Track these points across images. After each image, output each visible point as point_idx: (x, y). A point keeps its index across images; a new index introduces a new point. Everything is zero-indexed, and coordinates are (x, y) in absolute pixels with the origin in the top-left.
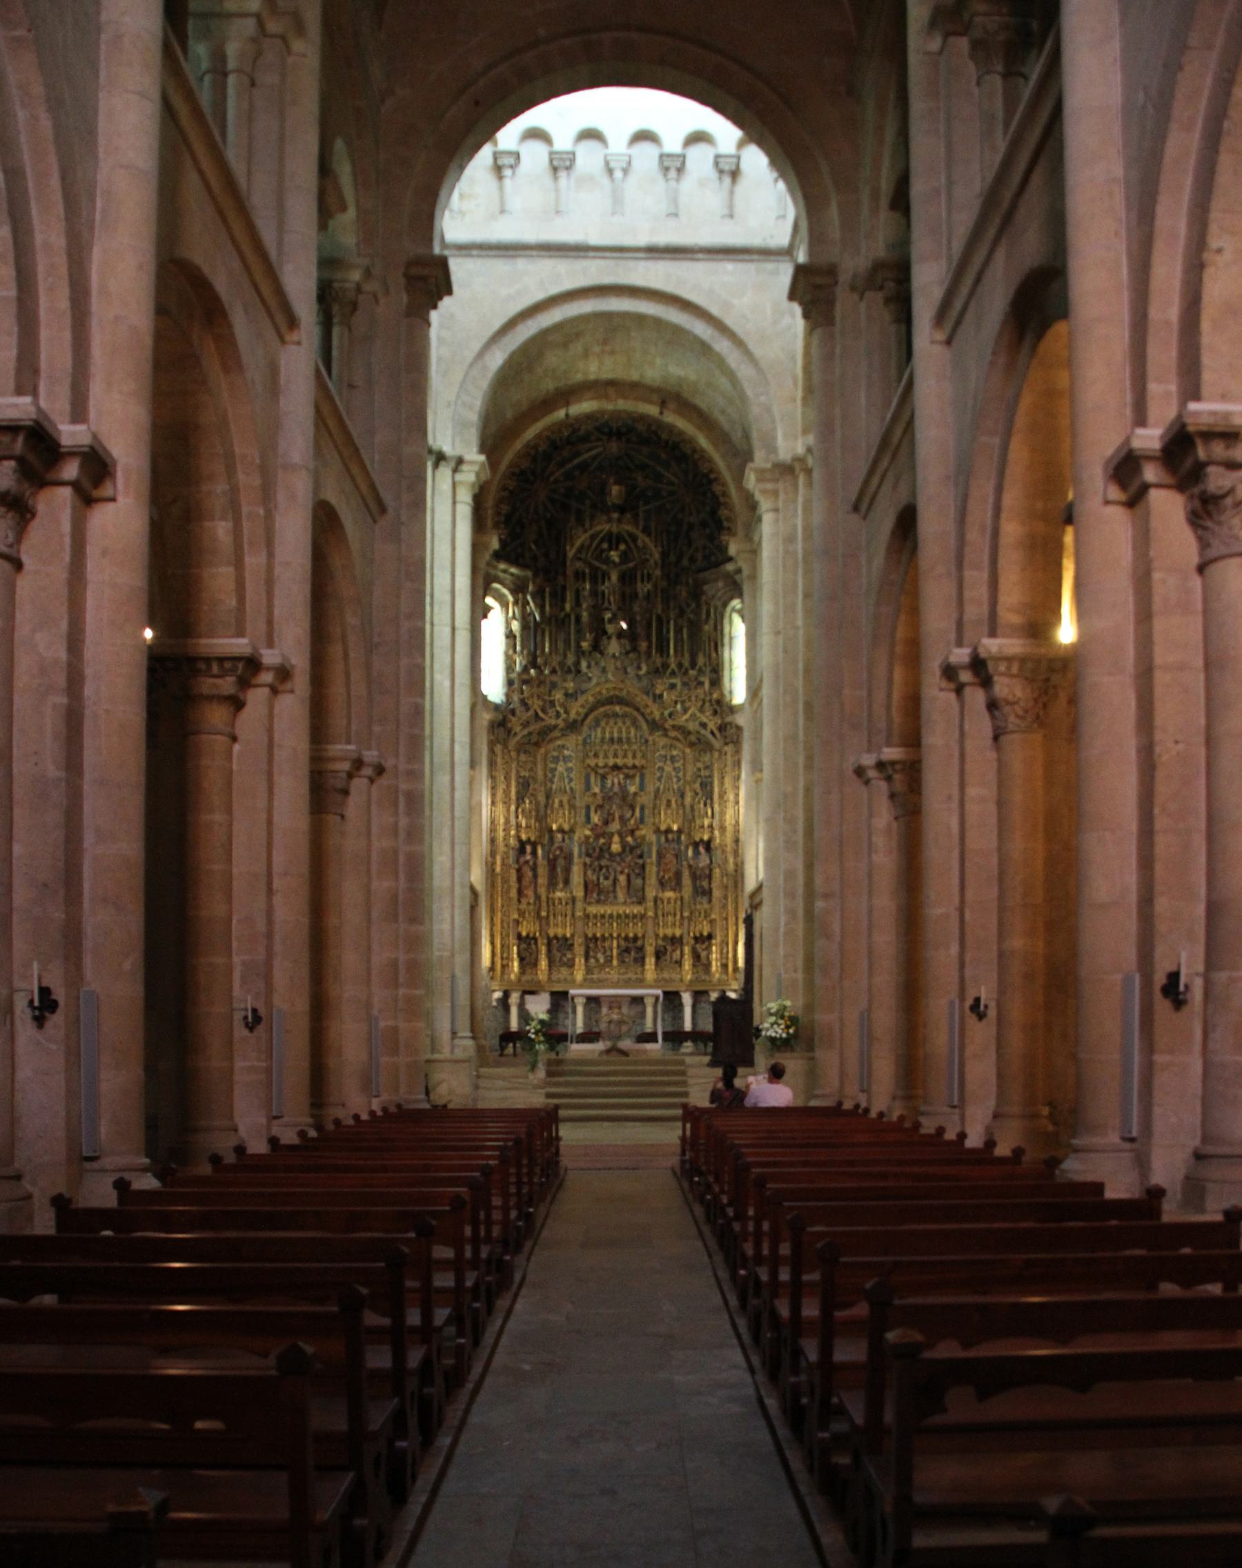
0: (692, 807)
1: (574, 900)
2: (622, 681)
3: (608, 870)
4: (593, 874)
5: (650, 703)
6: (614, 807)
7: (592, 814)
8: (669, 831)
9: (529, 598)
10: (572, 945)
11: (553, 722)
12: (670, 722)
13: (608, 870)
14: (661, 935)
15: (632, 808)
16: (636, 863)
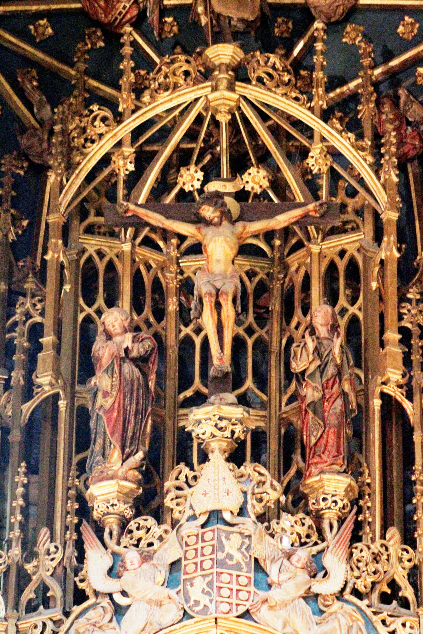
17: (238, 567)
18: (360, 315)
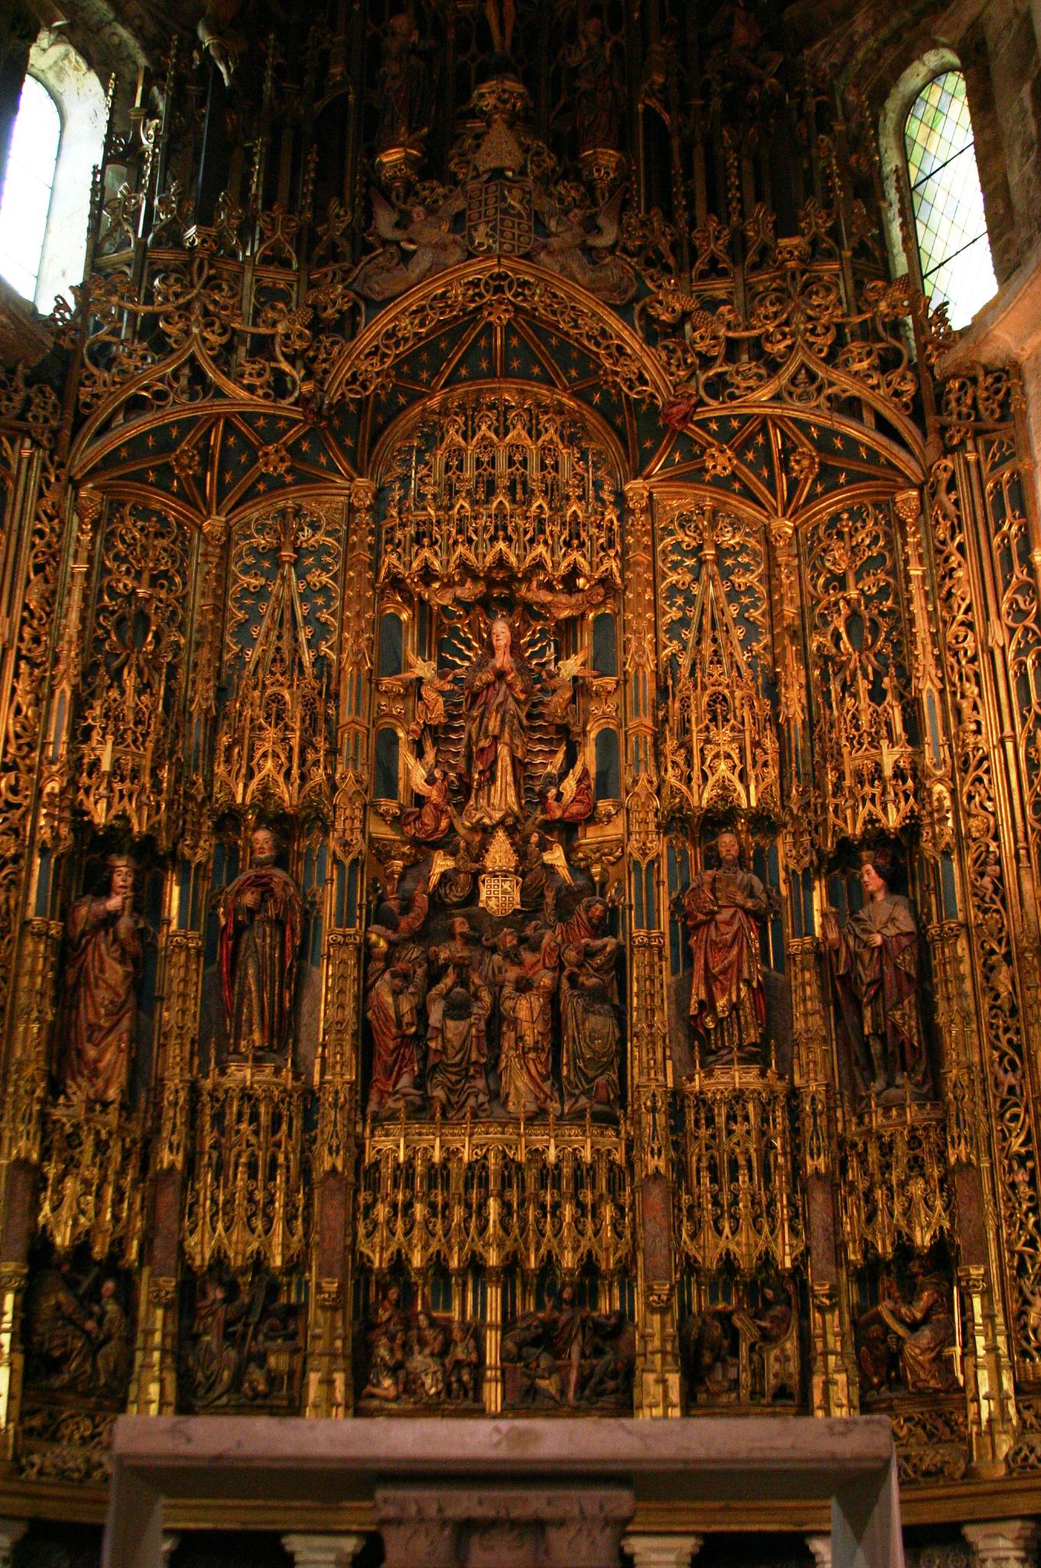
0: (810, 724)
1: (310, 1099)
2: (527, 256)
3: (463, 981)
4: (396, 993)
5: (633, 343)
6: (493, 724)
7: (406, 758)
8: (722, 817)
9: (201, 32)
10: (296, 1311)
11: (258, 403)
12: (714, 408)
13: (463, 981)
14: (710, 1260)
15: (568, 738)
16: (588, 953)
17: (519, 216)
18: (623, 42)
